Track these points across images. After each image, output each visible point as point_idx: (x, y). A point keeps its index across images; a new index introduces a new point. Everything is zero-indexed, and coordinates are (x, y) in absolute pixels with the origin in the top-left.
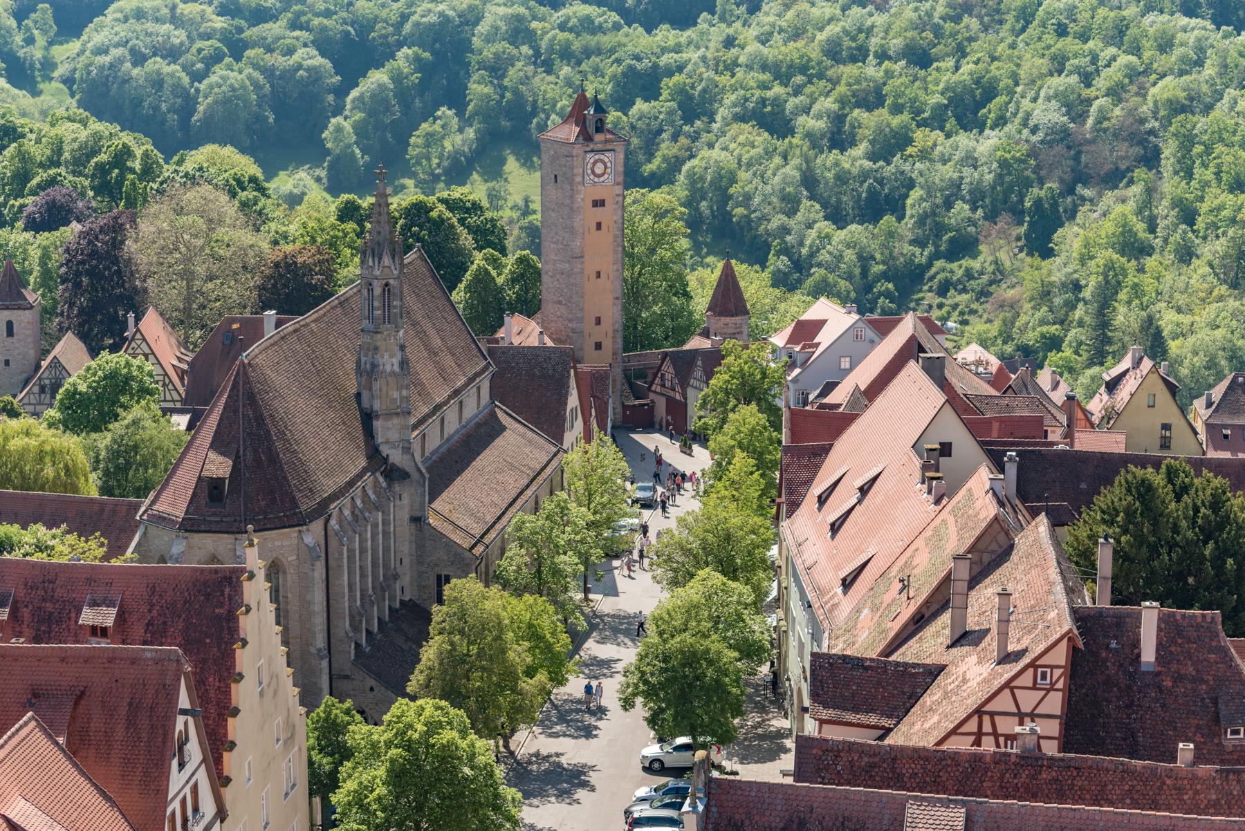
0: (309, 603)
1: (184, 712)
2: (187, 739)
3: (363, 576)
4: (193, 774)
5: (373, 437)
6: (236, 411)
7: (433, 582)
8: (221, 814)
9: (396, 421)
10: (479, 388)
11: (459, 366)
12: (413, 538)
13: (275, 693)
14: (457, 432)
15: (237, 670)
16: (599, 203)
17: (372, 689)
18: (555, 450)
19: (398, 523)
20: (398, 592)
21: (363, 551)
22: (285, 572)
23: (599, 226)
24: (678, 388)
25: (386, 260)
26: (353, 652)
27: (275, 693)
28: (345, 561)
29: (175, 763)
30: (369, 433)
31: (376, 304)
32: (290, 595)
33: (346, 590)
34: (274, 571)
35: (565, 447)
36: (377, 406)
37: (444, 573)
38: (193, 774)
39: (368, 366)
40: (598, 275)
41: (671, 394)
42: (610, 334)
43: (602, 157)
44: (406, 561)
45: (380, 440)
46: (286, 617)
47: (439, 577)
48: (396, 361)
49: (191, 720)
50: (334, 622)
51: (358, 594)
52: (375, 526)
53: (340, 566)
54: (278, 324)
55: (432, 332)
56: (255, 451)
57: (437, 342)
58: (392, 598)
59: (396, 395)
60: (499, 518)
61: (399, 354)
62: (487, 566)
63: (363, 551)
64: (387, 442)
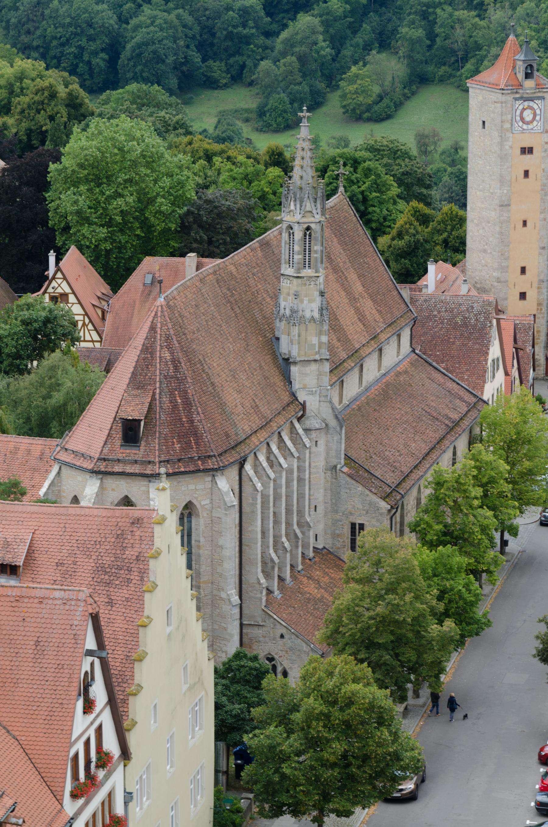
0: (221, 547)
1: (90, 653)
2: (93, 679)
3: (276, 522)
4: (98, 716)
5: (291, 383)
6: (152, 354)
7: (347, 530)
8: (125, 754)
9: (314, 367)
10: (399, 336)
11: (380, 312)
12: (329, 484)
13: (184, 637)
15: (146, 613)
16: (527, 151)
17: (282, 636)
18: (474, 400)
19: (313, 470)
20: (312, 540)
21: (277, 497)
22: (198, 515)
23: (526, 174)
25: (308, 205)
26: (264, 599)
27: (184, 637)
28: (259, 506)
29: (80, 704)
30: (288, 380)
31: (297, 248)
32: (202, 539)
33: (259, 536)
34: (187, 513)
35: (485, 398)
36: (295, 353)
37: (358, 521)
38: (98, 716)
39: (288, 312)
40: (525, 223)
42: (535, 285)
43: (531, 104)
44: (320, 509)
45: (296, 386)
46: (198, 562)
47: (353, 525)
48: (316, 306)
49: (97, 662)
50: (246, 567)
52: (290, 471)
53: (253, 512)
54: (199, 267)
55: (353, 277)
56: (172, 393)
57: (358, 288)
58: (305, 546)
59: (315, 340)
60: (416, 467)
62: (402, 517)
63: (277, 497)
64: (304, 387)
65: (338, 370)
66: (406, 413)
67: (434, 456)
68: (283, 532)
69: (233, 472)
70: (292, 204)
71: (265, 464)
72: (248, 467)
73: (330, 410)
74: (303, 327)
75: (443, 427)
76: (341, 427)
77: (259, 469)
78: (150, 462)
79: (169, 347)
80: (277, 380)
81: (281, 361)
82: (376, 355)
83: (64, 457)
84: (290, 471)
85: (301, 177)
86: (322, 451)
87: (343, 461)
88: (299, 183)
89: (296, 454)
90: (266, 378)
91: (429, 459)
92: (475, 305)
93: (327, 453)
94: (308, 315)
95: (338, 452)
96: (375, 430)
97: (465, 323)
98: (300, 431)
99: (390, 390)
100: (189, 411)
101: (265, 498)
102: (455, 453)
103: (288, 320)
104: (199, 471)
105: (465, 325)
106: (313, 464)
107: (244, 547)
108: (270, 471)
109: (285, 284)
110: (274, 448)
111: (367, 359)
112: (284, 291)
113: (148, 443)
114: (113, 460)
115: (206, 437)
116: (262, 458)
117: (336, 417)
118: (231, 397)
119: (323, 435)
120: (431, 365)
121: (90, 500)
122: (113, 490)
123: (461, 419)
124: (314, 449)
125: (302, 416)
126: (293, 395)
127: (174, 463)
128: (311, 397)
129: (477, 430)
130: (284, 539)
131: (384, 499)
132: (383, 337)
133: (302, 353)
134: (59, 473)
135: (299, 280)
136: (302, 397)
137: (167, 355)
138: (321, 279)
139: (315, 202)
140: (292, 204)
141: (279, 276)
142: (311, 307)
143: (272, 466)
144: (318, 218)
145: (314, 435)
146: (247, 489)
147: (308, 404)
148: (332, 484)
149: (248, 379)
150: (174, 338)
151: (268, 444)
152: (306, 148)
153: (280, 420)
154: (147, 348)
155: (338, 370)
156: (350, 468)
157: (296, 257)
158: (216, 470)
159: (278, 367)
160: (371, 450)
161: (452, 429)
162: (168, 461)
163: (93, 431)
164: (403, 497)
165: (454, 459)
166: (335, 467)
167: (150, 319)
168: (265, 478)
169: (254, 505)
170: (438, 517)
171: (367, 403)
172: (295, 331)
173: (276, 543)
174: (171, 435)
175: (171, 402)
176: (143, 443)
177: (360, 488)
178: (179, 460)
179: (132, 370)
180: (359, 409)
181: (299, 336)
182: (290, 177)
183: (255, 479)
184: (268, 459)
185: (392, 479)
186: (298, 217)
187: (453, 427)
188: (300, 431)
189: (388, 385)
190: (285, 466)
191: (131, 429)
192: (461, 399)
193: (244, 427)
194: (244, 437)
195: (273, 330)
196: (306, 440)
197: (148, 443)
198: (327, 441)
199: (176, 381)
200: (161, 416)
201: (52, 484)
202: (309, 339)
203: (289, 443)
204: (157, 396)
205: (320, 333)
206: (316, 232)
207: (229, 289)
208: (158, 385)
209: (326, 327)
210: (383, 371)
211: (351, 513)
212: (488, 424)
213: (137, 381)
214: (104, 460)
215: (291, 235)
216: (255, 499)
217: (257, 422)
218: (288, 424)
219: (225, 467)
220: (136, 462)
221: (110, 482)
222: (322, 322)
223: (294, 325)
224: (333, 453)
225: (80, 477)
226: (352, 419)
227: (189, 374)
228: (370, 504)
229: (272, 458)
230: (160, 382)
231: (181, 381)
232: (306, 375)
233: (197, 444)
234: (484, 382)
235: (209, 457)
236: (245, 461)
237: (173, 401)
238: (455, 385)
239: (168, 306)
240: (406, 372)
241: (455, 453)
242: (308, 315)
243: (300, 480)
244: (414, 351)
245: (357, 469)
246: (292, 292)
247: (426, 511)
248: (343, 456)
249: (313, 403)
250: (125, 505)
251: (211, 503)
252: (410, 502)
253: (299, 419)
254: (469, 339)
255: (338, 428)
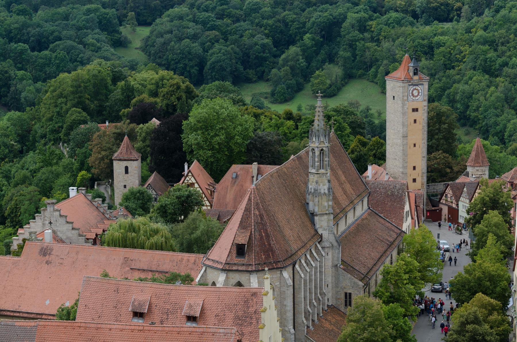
0: (285, 305)
3: (310, 293)
5: (315, 225)
6: (250, 212)
9: (326, 217)
10: (363, 201)
14: (353, 223)
19: (326, 267)
24: (454, 201)
28: (303, 285)
30: (313, 223)
33: (303, 300)
36: (316, 210)
37: (349, 292)
39: (313, 191)
41: (450, 204)
45: (317, 226)
48: (326, 187)
50: (296, 315)
51: (308, 302)
52: (316, 268)
53: (300, 288)
56: (260, 231)
59: (326, 204)
60: (375, 265)
61: (327, 184)
64: (321, 227)
65: (337, 218)
66: (368, 238)
67: (383, 259)
68: (313, 298)
69: (290, 269)
70: (314, 138)
71: (305, 265)
72: (297, 266)
73: (334, 238)
74: (320, 197)
75: (386, 245)
76: (339, 246)
77: (302, 267)
78: (250, 265)
79: (258, 209)
80: (308, 223)
81: (309, 214)
82: (352, 211)
83: (208, 263)
84: (316, 268)
85: (318, 125)
86: (330, 258)
87: (340, 262)
88: (317, 128)
89: (319, 260)
90: (303, 223)
91: (381, 261)
92: (397, 185)
93: (333, 259)
94: (322, 191)
95: (338, 258)
96: (354, 247)
97: (392, 194)
98: (320, 248)
99: (359, 228)
100: (269, 240)
101: (305, 281)
102: (391, 258)
103: (313, 194)
104: (274, 268)
105: (392, 195)
106: (326, 264)
107: (295, 305)
108: (307, 268)
109: (311, 177)
110: (308, 257)
111: (349, 213)
112: (311, 180)
113: (249, 256)
114: (232, 264)
115: (277, 252)
116: (303, 262)
117: (337, 241)
118: (288, 232)
119: (331, 250)
120: (378, 215)
121: (221, 284)
122: (232, 278)
123: (394, 241)
124: (326, 257)
125: (321, 241)
126: (316, 231)
127: (262, 265)
128: (324, 231)
129: (401, 246)
130: (314, 301)
131: (361, 281)
132: (355, 202)
133: (320, 210)
134: (205, 271)
135: (318, 175)
136: (320, 231)
137: (257, 212)
138: (328, 174)
139: (325, 137)
140: (314, 138)
141: (307, 174)
142: (324, 188)
143: (308, 266)
144: (327, 145)
145: (326, 250)
146: (297, 277)
147: (323, 235)
148: (335, 273)
149: (295, 223)
150: (260, 204)
151: (305, 255)
152: (320, 111)
153: (311, 243)
154: (247, 209)
155: (337, 218)
156: (344, 266)
157: (316, 164)
158: (282, 268)
159: (308, 217)
160: (353, 257)
161: (390, 246)
162: (259, 264)
163: (221, 250)
164: (370, 279)
165: (391, 260)
166: (337, 265)
167: (248, 195)
168: (305, 271)
169: (300, 284)
170: (387, 289)
171: (349, 234)
172: (316, 200)
173: (310, 302)
174: (260, 252)
175: (260, 235)
176: (247, 256)
177: (349, 275)
178: (264, 263)
179: (240, 220)
180: (346, 237)
181: (318, 202)
182: (313, 125)
183: (301, 272)
184: (306, 262)
185: (364, 271)
186: (317, 144)
187: (390, 245)
188: (320, 248)
189: (358, 225)
190: (314, 265)
191: (241, 249)
192: (393, 231)
193: (294, 247)
194: (295, 252)
195: (305, 199)
196: (323, 253)
197: (249, 256)
198: (333, 253)
199: (261, 225)
200: (255, 242)
201: (202, 276)
202: (323, 203)
203: (315, 254)
204: (253, 233)
205: (328, 201)
206: (326, 152)
207: (284, 180)
208: (253, 227)
209: (331, 198)
210: (356, 218)
211: (345, 288)
212: (407, 244)
213: (243, 225)
214: (228, 264)
215: (314, 153)
216: (300, 282)
217: (300, 244)
218: (314, 245)
219: (286, 266)
220: (243, 265)
221: (231, 275)
222: (329, 195)
223: (316, 197)
224: (335, 259)
225: (216, 272)
226: (344, 241)
227: (268, 221)
228: (354, 283)
229: (307, 261)
230: (254, 226)
231: (264, 225)
232: (322, 221)
233: (273, 255)
234: (403, 223)
235: (279, 261)
236: (295, 263)
237: (260, 235)
238: (390, 224)
239: (257, 189)
240: (366, 218)
241: (391, 258)
242: (322, 191)
243: (321, 272)
244: (369, 208)
245: (347, 266)
246: (314, 181)
247: (381, 286)
248: (340, 260)
249: (325, 234)
250: (238, 286)
251: (280, 284)
252: (372, 282)
253: (319, 243)
254: (395, 202)
255: (338, 247)
